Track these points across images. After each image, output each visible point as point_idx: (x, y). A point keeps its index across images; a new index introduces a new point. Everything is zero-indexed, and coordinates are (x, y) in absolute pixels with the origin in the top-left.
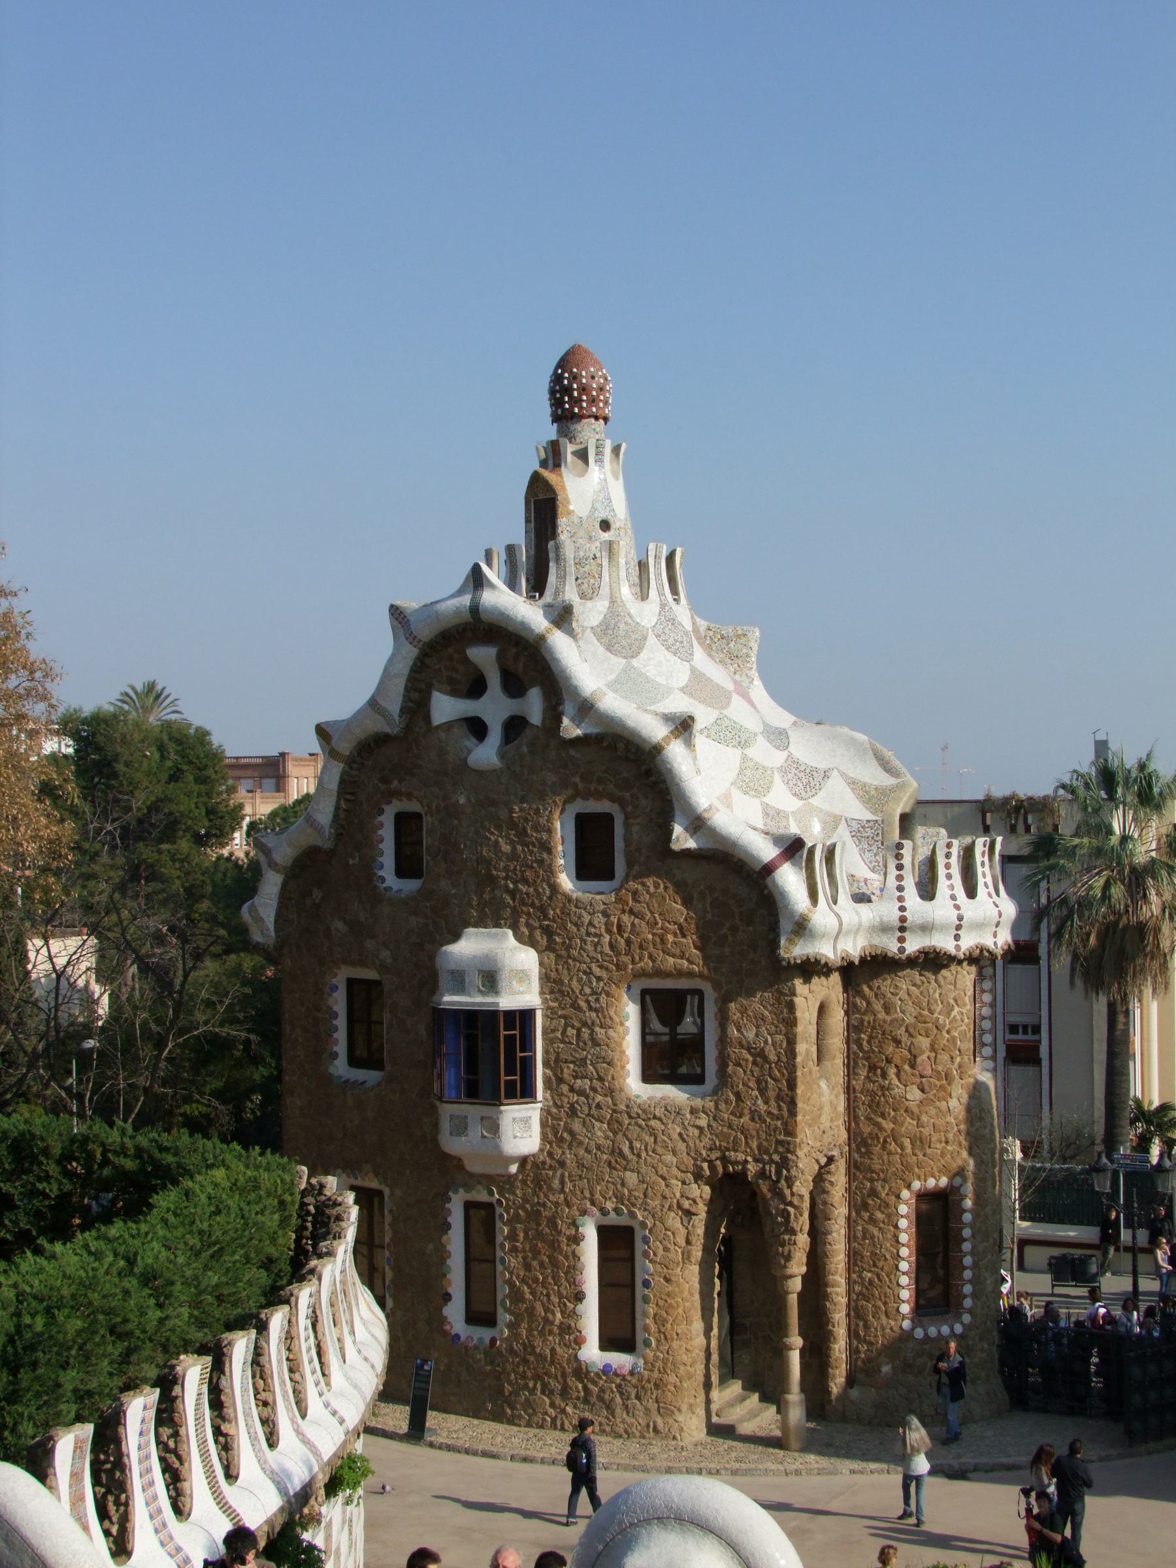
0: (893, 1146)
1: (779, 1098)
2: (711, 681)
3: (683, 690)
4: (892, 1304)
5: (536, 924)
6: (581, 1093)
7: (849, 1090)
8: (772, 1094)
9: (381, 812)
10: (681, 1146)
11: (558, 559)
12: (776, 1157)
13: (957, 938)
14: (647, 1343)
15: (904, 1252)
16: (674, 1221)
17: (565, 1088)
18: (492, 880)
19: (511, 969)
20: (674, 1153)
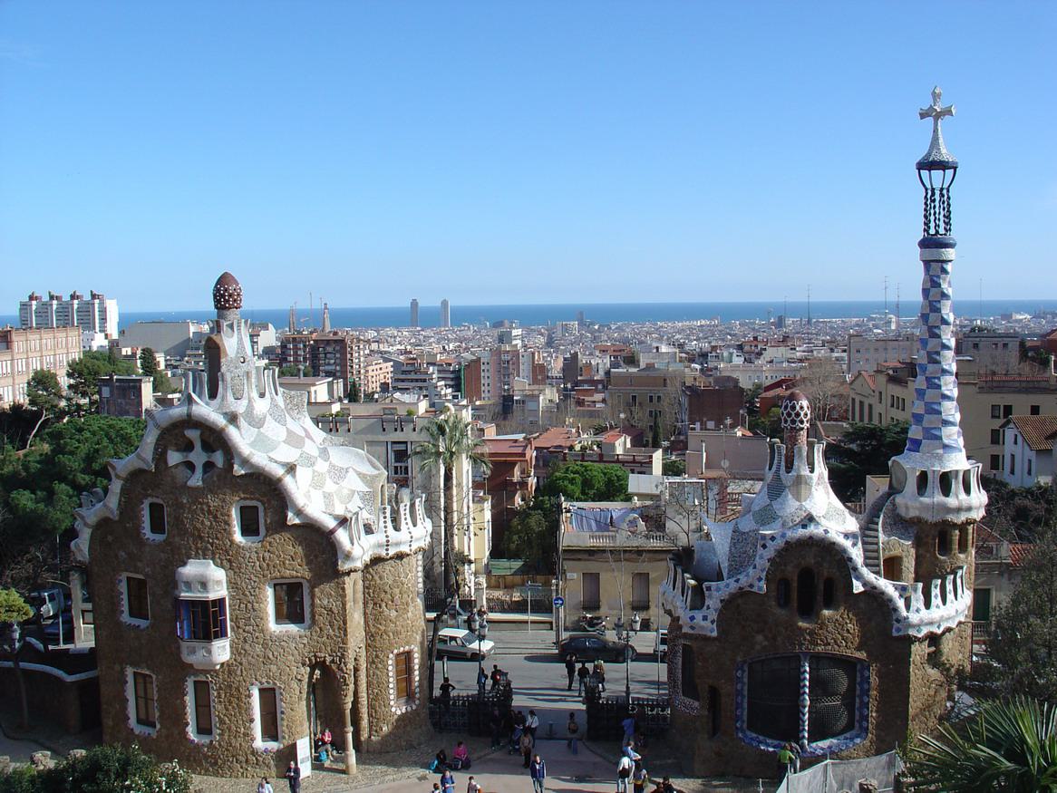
0: (385, 636)
1: (339, 628)
2: (295, 434)
3: (284, 442)
4: (387, 702)
5: (224, 558)
6: (248, 632)
7: (365, 614)
8: (336, 627)
9: (143, 503)
10: (296, 652)
11: (223, 380)
12: (339, 654)
13: (410, 546)
14: (284, 738)
15: (391, 680)
16: (294, 685)
17: (241, 631)
18: (201, 538)
19: (210, 578)
20: (293, 655)
